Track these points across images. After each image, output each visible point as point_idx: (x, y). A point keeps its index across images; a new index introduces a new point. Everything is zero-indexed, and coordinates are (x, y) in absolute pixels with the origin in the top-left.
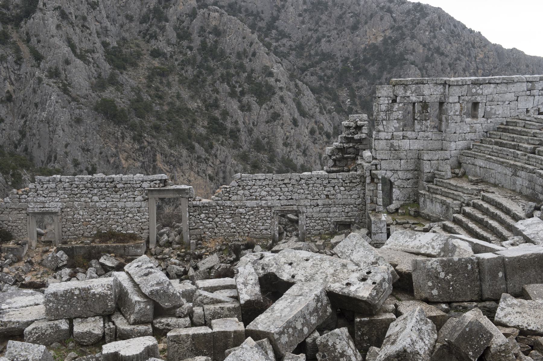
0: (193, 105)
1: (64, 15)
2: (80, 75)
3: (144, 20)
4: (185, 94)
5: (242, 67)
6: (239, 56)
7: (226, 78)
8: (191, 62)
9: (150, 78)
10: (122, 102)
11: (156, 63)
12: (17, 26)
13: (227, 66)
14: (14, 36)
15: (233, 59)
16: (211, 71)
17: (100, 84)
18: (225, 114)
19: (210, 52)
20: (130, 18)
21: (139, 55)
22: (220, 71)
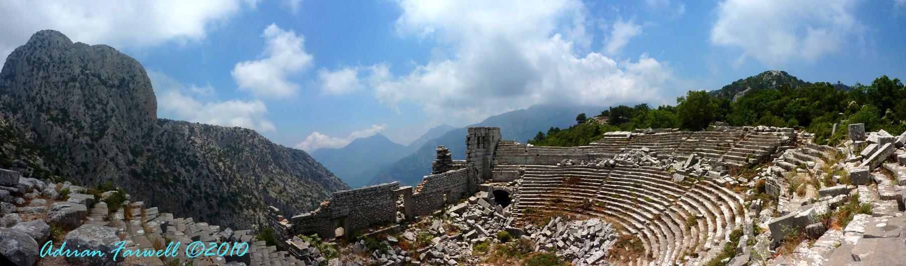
0: (166, 171)
1: (115, 137)
2: (122, 160)
3: (143, 137)
4: (162, 166)
5: (185, 155)
6: (184, 150)
7: (178, 159)
8: (163, 153)
9: (148, 160)
10: (139, 170)
11: (149, 154)
12: (97, 141)
13: (179, 154)
14: (96, 146)
15: (180, 151)
16: (172, 157)
17: (129, 163)
18: (180, 174)
19: (172, 149)
20: (138, 137)
21: (143, 151)
22: (175, 157)
